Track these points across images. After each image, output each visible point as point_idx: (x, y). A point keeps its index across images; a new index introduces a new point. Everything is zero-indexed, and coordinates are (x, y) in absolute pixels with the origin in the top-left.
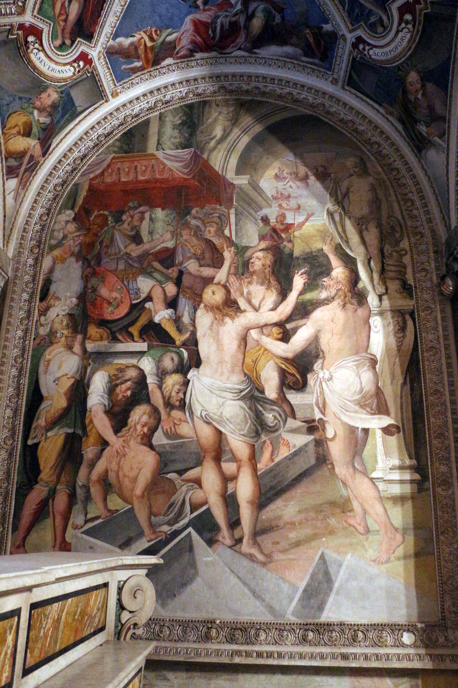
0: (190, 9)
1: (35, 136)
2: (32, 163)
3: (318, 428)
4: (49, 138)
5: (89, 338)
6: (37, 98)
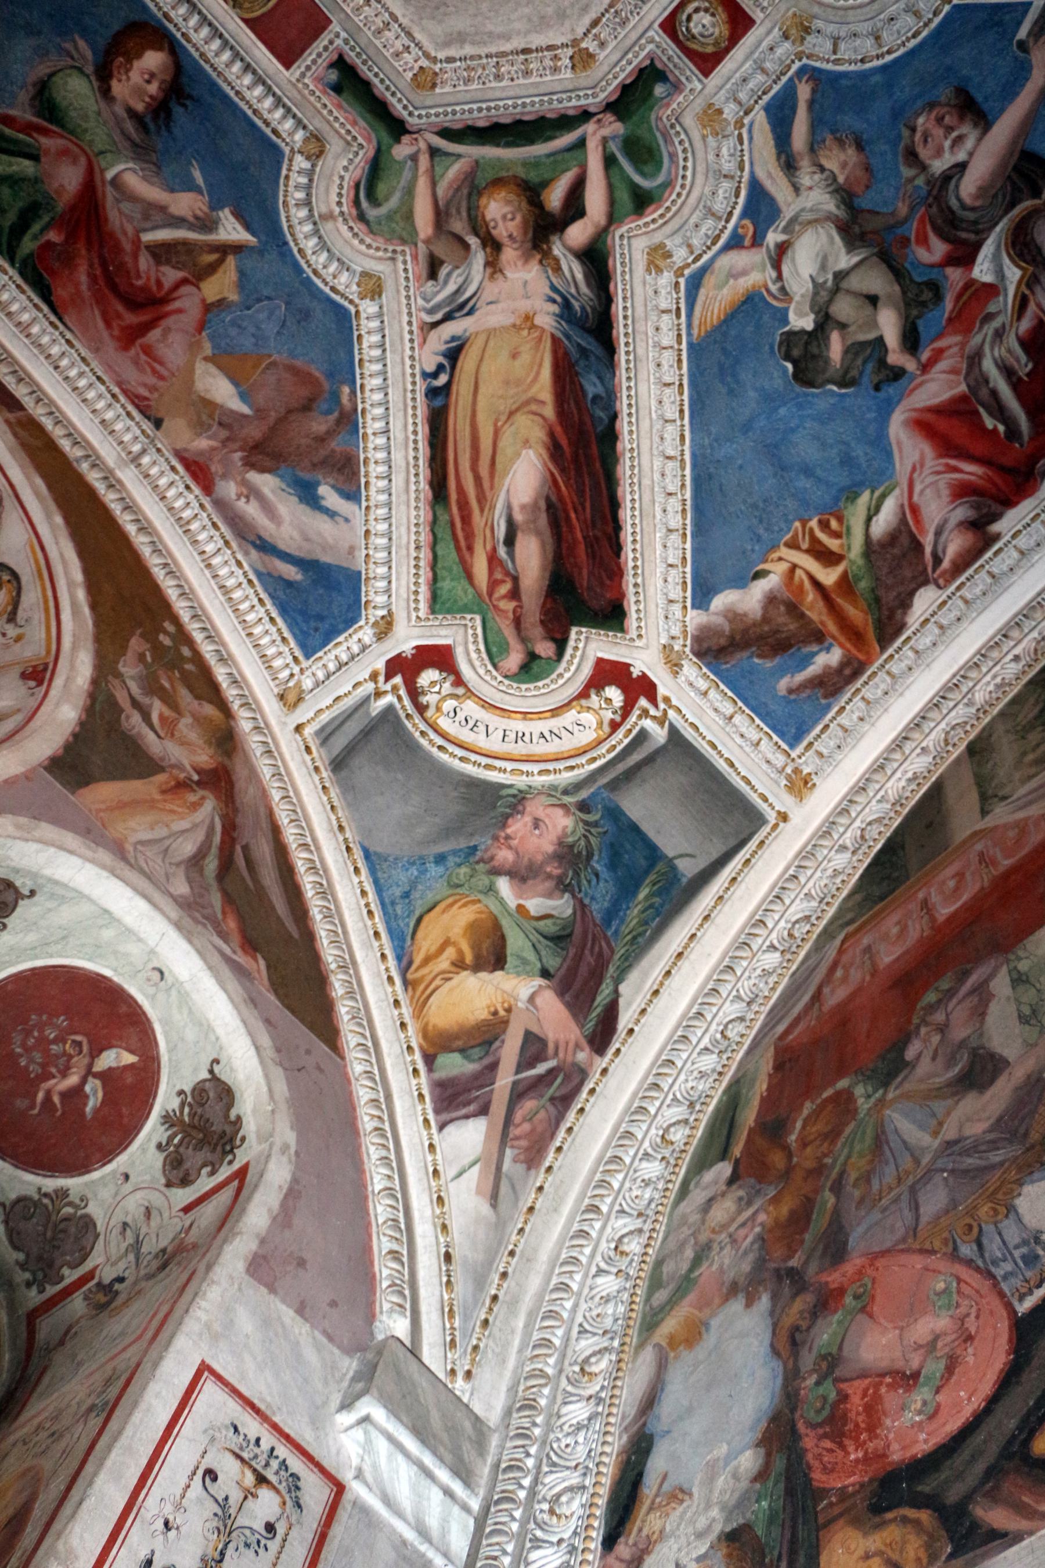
0: (882, 395)
1: (525, 962)
2: (541, 1069)
4: (597, 976)
6: (496, 838)
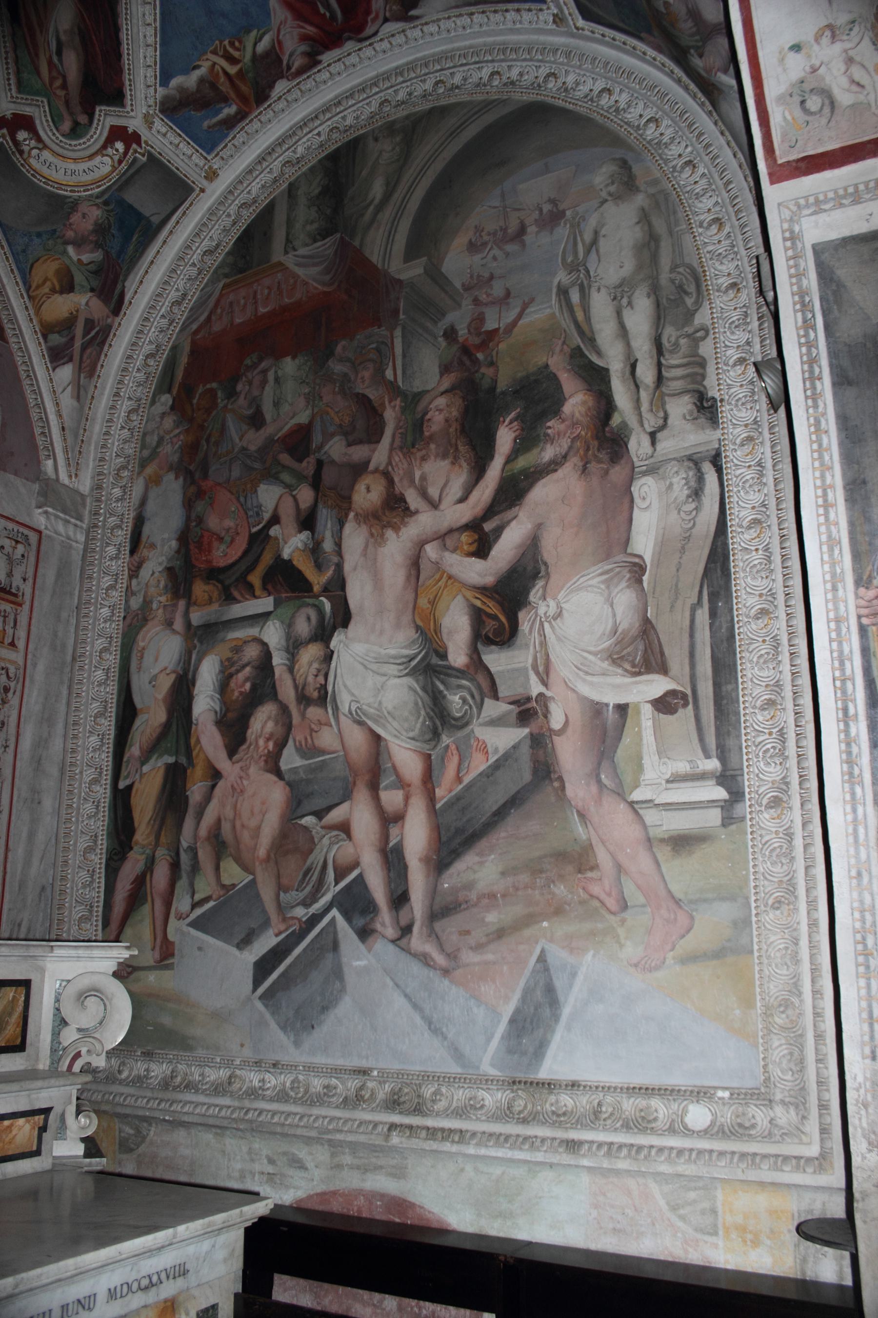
1: (83, 287)
2: (93, 333)
3: (536, 713)
4: (115, 282)
5: (195, 604)
6: (65, 225)
